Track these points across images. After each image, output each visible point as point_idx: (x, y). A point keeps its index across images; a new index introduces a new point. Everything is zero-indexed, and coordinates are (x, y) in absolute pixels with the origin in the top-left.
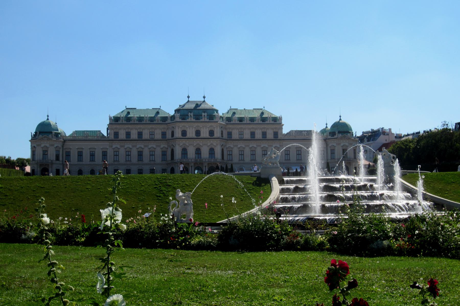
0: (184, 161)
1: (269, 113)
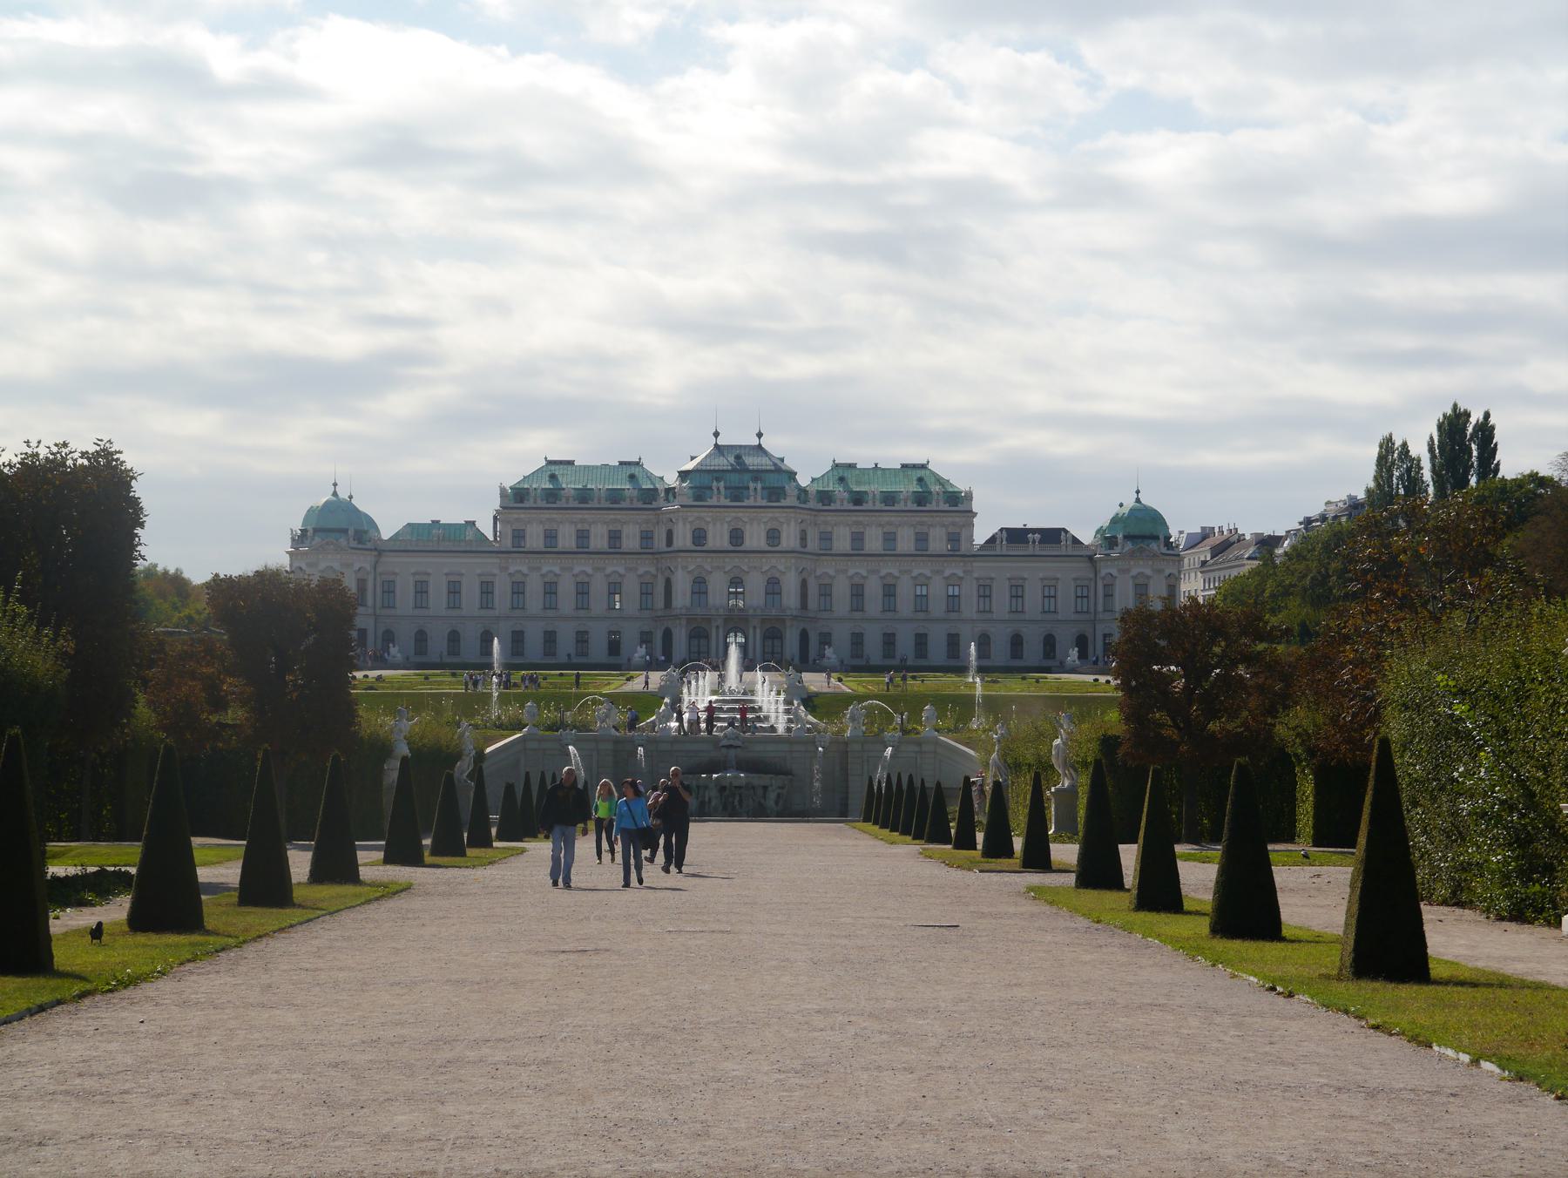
0: (698, 611)
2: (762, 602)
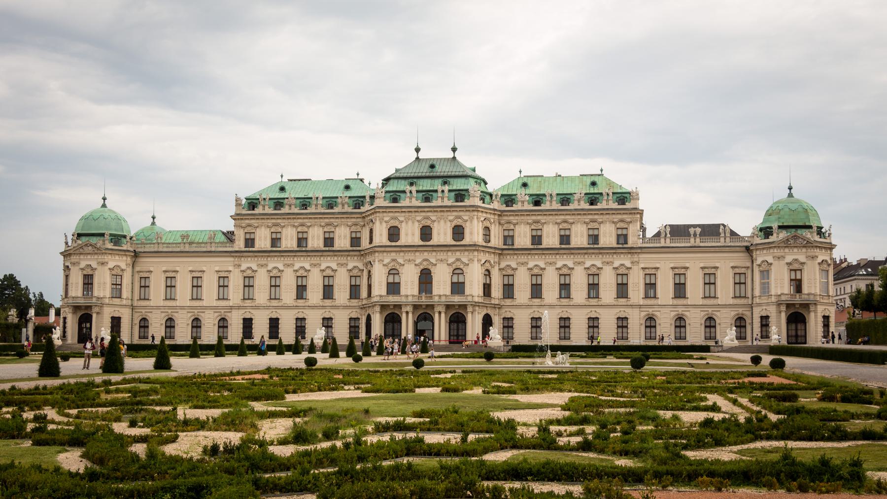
1: (610, 184)
2: (448, 291)
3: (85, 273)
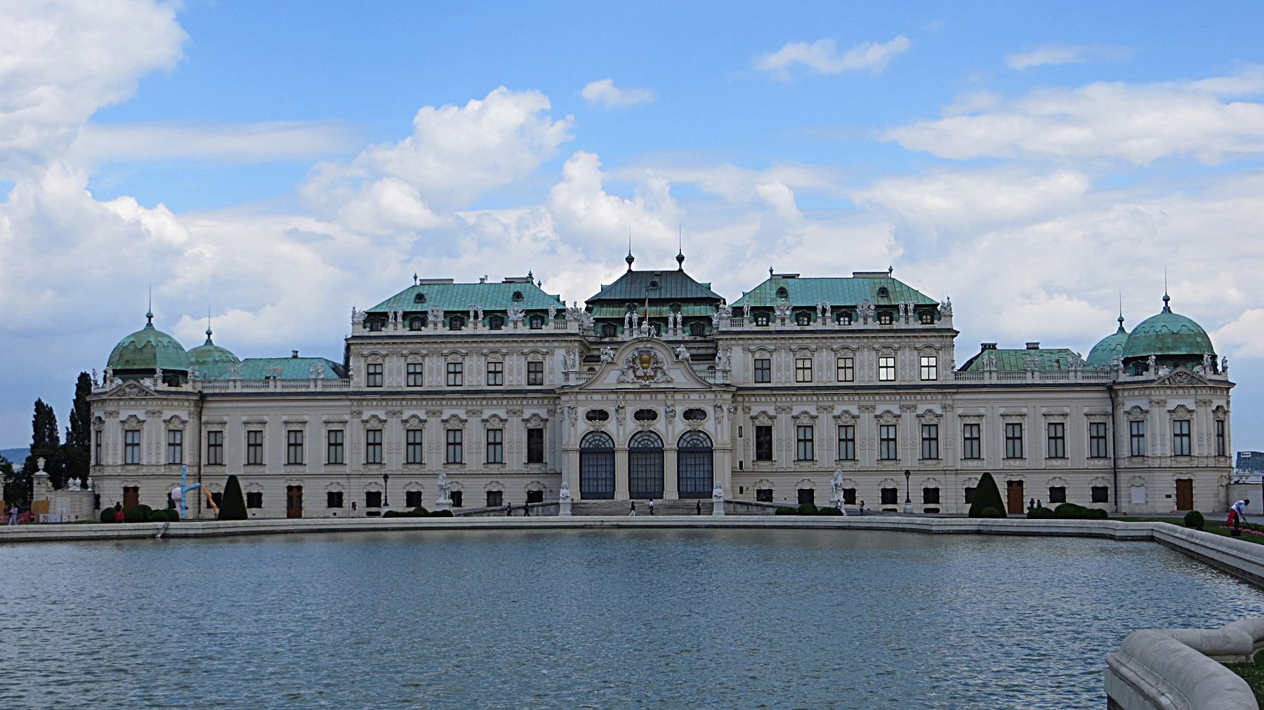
3: (126, 427)
